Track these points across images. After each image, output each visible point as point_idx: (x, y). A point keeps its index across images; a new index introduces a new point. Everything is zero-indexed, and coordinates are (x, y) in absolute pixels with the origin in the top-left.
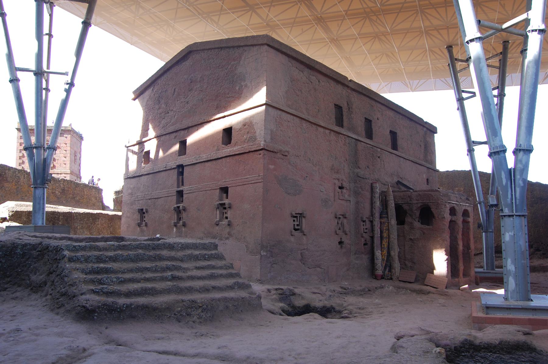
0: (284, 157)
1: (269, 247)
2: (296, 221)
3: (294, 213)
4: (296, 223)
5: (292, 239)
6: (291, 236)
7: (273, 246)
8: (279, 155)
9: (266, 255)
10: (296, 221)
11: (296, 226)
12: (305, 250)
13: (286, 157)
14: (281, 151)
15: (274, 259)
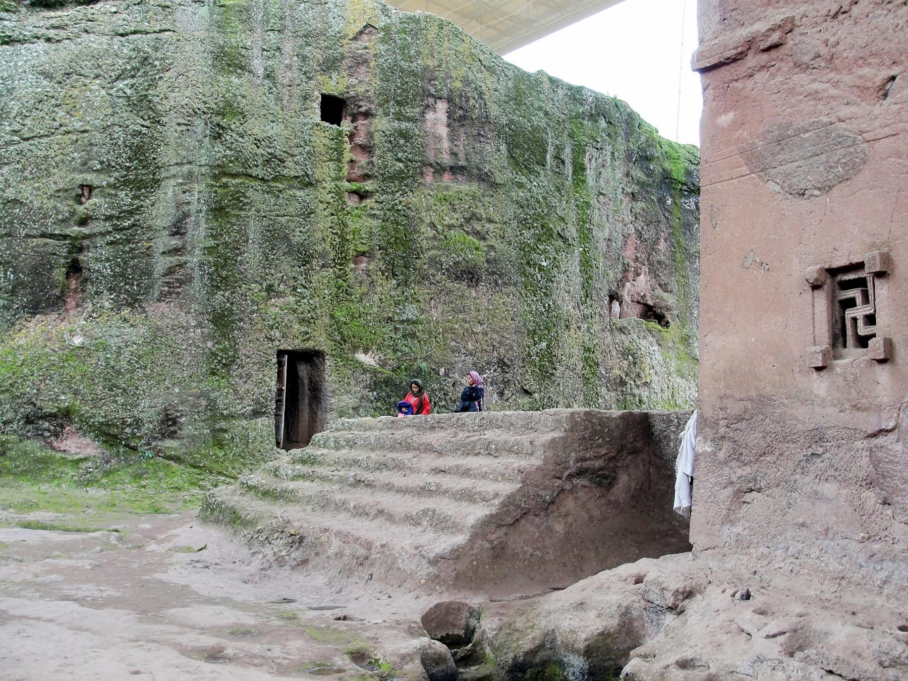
0: (774, 53)
1: (722, 422)
2: (859, 301)
3: (812, 271)
4: (859, 312)
5: (820, 385)
6: (815, 375)
7: (740, 419)
8: (752, 61)
9: (714, 454)
10: (859, 301)
11: (860, 323)
12: (892, 437)
13: (782, 51)
14: (750, 43)
15: (747, 470)
